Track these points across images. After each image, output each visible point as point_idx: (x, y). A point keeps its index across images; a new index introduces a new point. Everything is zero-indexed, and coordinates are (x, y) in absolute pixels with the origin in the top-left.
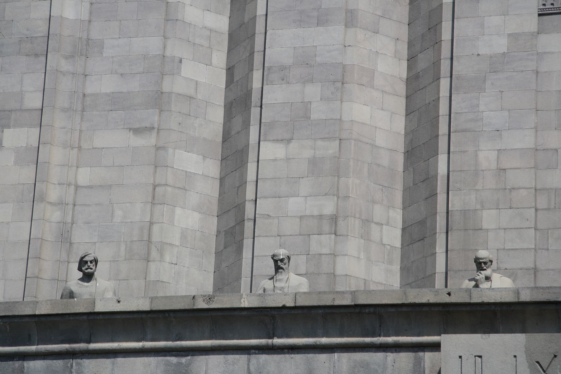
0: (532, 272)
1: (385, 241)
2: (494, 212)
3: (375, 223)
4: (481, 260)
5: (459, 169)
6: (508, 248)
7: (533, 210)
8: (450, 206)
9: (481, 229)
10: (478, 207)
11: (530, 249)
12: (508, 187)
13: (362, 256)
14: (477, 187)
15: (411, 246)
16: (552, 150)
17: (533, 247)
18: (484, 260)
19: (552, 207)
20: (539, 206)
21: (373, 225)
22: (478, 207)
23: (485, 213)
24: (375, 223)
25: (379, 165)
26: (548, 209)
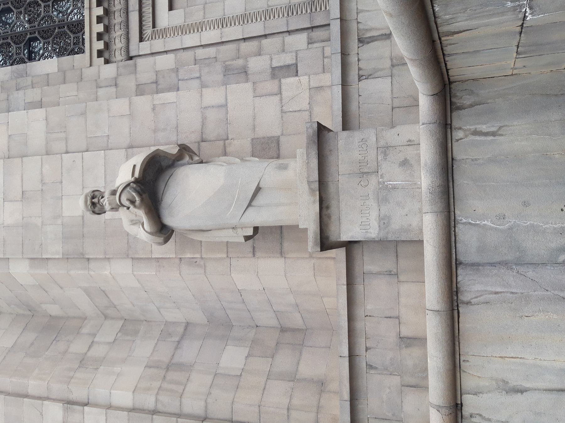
0: (130, 150)
1: (111, 339)
2: (64, 202)
3: (88, 350)
4: (89, 202)
5: (21, 246)
6: (103, 183)
7: (64, 156)
8: (57, 257)
9: (83, 217)
10: (59, 222)
11: (105, 156)
12: (40, 186)
13: (117, 369)
14: (39, 224)
15: (118, 307)
16: (9, 142)
17: (103, 152)
18: (89, 198)
19: (63, 135)
20: (64, 150)
21: (89, 354)
22: (59, 222)
23: (66, 213)
24: (88, 350)
25: (32, 344)
26: (66, 139)
